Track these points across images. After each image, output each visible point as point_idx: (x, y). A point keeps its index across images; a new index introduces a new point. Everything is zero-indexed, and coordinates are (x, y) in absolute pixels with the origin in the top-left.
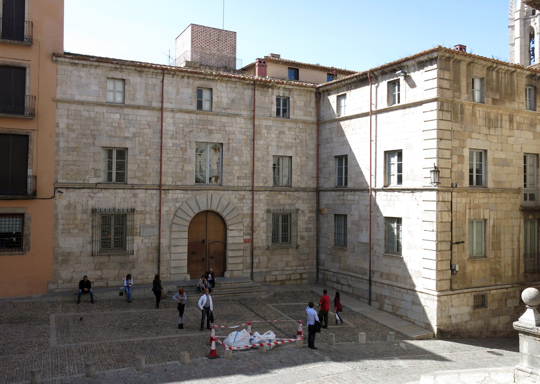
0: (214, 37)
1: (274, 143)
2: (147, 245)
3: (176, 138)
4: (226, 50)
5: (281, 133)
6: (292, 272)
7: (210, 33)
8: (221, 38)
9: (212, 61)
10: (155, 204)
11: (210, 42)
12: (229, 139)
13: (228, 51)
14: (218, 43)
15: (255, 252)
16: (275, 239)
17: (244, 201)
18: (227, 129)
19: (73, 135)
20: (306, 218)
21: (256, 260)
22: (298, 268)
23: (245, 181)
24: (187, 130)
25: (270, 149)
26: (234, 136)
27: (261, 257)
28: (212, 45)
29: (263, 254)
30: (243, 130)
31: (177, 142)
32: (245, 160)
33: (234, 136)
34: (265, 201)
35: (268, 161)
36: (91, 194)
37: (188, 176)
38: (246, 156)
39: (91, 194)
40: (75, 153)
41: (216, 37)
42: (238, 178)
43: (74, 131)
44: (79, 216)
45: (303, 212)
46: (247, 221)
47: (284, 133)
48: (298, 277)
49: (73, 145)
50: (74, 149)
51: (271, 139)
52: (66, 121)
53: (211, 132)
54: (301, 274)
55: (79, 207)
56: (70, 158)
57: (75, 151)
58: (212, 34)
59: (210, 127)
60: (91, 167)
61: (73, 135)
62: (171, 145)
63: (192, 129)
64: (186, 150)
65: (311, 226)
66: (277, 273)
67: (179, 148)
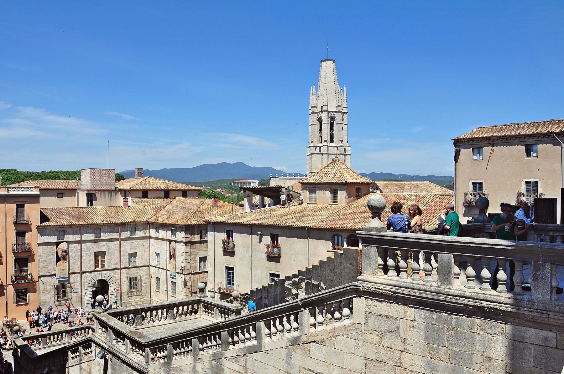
0: (103, 173)
1: (129, 248)
2: (76, 296)
3: (86, 251)
4: (109, 180)
5: (131, 243)
6: (139, 301)
7: (100, 172)
8: (106, 174)
9: (102, 187)
10: (79, 279)
11: (100, 176)
12: (109, 249)
13: (111, 180)
14: (105, 177)
15: (122, 294)
16: (130, 289)
17: (116, 274)
18: (108, 244)
19: (45, 255)
20: (144, 278)
21: (122, 298)
22: (141, 299)
23: (116, 265)
24: (91, 247)
25: (127, 251)
26: (111, 247)
27: (124, 296)
28: (102, 178)
29: (125, 295)
30: (115, 244)
31: (87, 253)
32: (116, 256)
33: (111, 247)
34: (126, 273)
35: (126, 256)
36: (52, 278)
37: (92, 266)
38: (117, 254)
39: (52, 278)
40: (46, 262)
41: (104, 174)
42: (113, 264)
43: (45, 254)
44: (48, 287)
45: (143, 275)
46: (118, 281)
47: (133, 243)
48: (142, 303)
49: (45, 259)
50: (45, 261)
51: (127, 246)
52: (42, 250)
53: (101, 247)
54: (143, 302)
55: (48, 284)
56: (44, 265)
57: (45, 262)
58: (101, 172)
59: (100, 245)
60: (52, 267)
61: (45, 255)
62: (84, 254)
63: (93, 247)
64: (90, 256)
65: (147, 281)
66: (132, 302)
67: (87, 255)
